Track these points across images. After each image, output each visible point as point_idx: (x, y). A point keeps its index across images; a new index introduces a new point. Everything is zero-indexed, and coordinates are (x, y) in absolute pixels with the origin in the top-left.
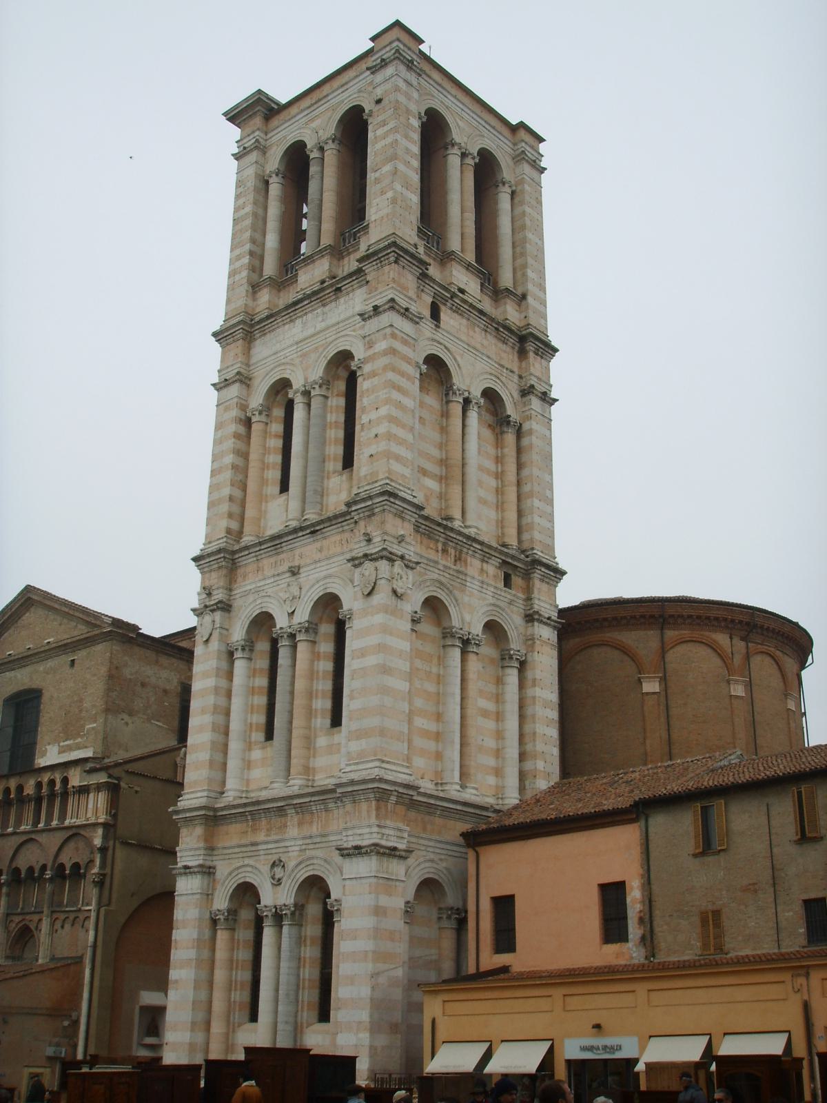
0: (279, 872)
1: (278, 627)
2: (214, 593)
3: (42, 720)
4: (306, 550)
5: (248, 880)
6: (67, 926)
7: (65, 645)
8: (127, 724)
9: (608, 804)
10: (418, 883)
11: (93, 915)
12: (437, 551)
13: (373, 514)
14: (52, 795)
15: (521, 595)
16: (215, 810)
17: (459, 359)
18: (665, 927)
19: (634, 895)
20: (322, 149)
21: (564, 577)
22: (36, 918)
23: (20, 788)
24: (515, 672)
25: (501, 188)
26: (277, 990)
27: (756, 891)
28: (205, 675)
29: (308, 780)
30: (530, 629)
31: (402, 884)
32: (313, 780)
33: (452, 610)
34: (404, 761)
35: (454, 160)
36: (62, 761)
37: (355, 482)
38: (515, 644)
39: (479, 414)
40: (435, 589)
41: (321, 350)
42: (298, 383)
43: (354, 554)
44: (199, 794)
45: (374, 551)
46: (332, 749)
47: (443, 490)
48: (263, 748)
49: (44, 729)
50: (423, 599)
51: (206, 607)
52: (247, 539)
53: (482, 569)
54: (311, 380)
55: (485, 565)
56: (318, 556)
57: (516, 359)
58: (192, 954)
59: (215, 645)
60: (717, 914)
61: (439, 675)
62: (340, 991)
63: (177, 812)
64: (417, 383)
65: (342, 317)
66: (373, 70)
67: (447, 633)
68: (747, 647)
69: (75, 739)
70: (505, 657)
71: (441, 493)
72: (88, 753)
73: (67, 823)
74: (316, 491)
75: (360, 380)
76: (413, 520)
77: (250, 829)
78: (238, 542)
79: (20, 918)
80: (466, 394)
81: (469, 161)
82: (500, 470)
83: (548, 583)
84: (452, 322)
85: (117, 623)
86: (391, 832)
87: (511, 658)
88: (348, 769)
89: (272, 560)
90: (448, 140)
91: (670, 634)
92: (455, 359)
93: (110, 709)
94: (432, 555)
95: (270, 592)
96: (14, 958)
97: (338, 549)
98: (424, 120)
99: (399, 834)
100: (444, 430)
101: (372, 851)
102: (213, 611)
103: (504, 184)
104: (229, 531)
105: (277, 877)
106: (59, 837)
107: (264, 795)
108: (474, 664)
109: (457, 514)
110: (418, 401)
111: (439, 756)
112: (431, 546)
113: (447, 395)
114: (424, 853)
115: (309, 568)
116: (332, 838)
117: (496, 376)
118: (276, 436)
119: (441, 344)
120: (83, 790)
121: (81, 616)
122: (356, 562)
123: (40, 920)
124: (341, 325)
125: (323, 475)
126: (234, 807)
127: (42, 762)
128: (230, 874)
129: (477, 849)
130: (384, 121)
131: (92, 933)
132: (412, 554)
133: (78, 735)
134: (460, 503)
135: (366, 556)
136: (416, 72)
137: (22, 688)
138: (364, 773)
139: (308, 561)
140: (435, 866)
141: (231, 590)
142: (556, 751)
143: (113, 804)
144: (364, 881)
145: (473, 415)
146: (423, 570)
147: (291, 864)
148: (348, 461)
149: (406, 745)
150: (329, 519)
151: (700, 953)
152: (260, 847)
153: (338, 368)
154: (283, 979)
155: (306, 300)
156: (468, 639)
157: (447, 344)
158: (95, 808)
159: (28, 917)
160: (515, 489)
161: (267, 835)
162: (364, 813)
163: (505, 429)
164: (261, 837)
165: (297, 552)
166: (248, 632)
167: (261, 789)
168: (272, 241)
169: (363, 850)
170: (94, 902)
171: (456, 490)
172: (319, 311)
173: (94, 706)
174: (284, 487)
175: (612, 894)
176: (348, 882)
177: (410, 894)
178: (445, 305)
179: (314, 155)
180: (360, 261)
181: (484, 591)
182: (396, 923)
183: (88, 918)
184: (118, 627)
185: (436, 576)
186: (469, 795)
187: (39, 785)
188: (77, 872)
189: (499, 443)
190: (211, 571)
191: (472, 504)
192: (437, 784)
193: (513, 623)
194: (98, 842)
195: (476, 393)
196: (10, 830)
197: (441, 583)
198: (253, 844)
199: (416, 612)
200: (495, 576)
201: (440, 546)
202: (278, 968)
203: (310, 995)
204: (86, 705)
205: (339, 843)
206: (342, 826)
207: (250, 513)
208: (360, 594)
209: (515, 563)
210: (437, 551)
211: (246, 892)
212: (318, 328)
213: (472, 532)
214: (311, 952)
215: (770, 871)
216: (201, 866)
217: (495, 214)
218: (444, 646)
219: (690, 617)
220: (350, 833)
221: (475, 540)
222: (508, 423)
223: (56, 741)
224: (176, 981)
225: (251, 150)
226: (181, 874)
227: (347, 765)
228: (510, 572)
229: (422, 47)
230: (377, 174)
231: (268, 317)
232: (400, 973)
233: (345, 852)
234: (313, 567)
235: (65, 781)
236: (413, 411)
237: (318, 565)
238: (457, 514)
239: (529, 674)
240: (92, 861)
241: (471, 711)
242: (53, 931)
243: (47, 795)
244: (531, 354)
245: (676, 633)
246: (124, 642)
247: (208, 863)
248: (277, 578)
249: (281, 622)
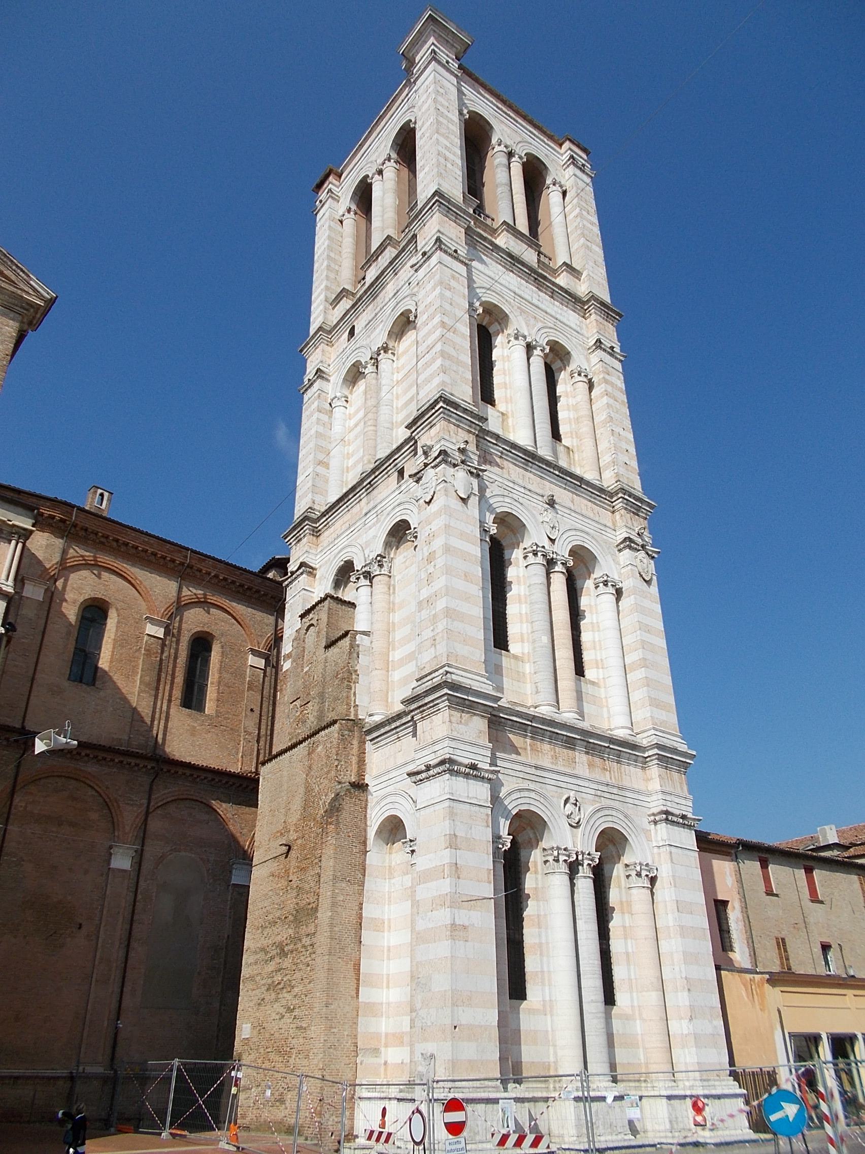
60: (783, 939)
77: (529, 748)
155: (527, 268)
237: (573, 514)
248: (528, 493)
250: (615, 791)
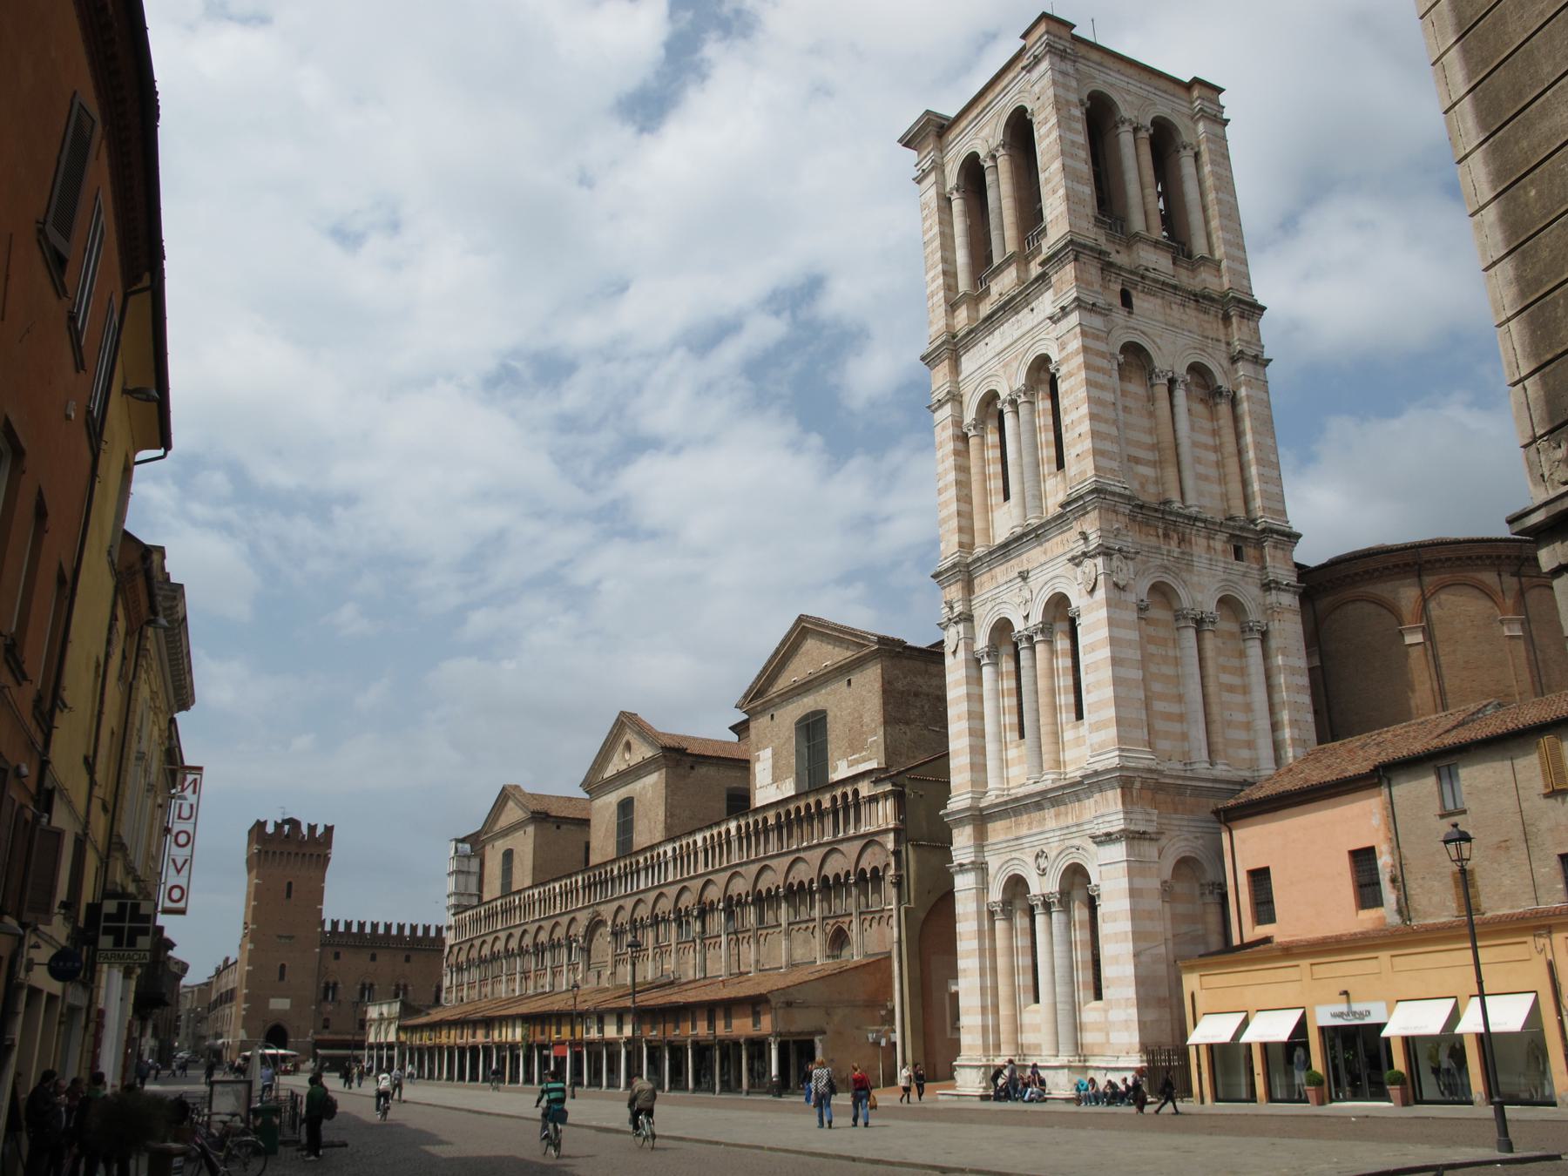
0: (1043, 863)
1: (1016, 631)
2: (955, 605)
3: (829, 738)
4: (1032, 557)
5: (1017, 872)
6: (874, 925)
7: (840, 667)
8: (905, 733)
9: (1352, 770)
10: (1174, 862)
11: (895, 913)
12: (1158, 537)
13: (1087, 513)
14: (846, 808)
15: (1255, 566)
16: (981, 810)
17: (1158, 340)
18: (1419, 890)
19: (1384, 861)
20: (994, 157)
21: (1300, 540)
22: (847, 919)
23: (819, 803)
24: (1257, 643)
25: (1183, 153)
26: (1053, 973)
27: (1508, 848)
28: (957, 684)
29: (1061, 774)
30: (1269, 598)
31: (1156, 866)
32: (1066, 774)
33: (1182, 592)
34: (1145, 746)
35: (1126, 137)
36: (850, 774)
37: (1068, 482)
38: (1254, 615)
39: (1188, 391)
40: (1159, 574)
41: (1020, 357)
42: (1004, 394)
43: (1074, 553)
44: (965, 796)
45: (1091, 548)
46: (1079, 742)
47: (1159, 475)
48: (1018, 746)
49: (833, 746)
50: (1149, 586)
51: (950, 620)
52: (979, 551)
53: (1209, 546)
54: (1015, 388)
55: (1211, 542)
56: (1043, 559)
57: (1221, 326)
58: (974, 944)
59: (961, 654)
61: (1176, 658)
62: (1107, 972)
63: (948, 815)
64: (1116, 374)
65: (1035, 323)
66: (1029, 69)
67: (1179, 615)
68: (1520, 583)
69: (861, 752)
70: (1245, 629)
71: (1157, 478)
72: (873, 765)
73: (862, 831)
74: (1034, 496)
75: (1059, 381)
76: (1127, 511)
78: (971, 554)
80: (1170, 375)
81: (1144, 134)
82: (1218, 443)
83: (1283, 549)
84: (1146, 305)
85: (882, 640)
86: (1139, 817)
87: (1251, 629)
88: (1092, 760)
89: (1003, 568)
90: (1117, 119)
91: (1427, 580)
92: (1154, 342)
93: (888, 721)
94: (1153, 541)
95: (1005, 598)
96: (833, 957)
97: (1061, 551)
98: (1088, 105)
99: (1148, 817)
100: (1152, 415)
101: (1121, 837)
102: (956, 623)
103: (1185, 148)
104: (961, 545)
105: (1042, 867)
106: (859, 844)
107: (1021, 792)
108: (1210, 642)
109: (1174, 496)
110: (1119, 393)
111: (1184, 737)
112: (1151, 532)
113: (1150, 378)
114: (1178, 833)
115: (1037, 571)
116: (1086, 827)
117: (1200, 349)
118: (993, 447)
119: (1136, 329)
120: (873, 799)
121: (850, 638)
122: (1076, 561)
123: (851, 921)
124: (1035, 330)
125: (1038, 479)
126: (997, 805)
127: (835, 776)
128: (1000, 868)
129: (1229, 824)
130: (1046, 118)
131: (895, 930)
132: (1130, 544)
133: (863, 749)
134: (1177, 484)
135: (1085, 554)
136: (1070, 59)
137: (809, 711)
138: (1106, 762)
139: (1036, 565)
140: (1190, 844)
141: (970, 601)
142: (1310, 717)
143: (900, 808)
144: (1118, 865)
145: (1180, 394)
146: (1144, 558)
147: (1052, 855)
148: (1060, 464)
149: (1145, 730)
150: (1048, 522)
151: (1456, 914)
152: (1024, 841)
153: (1039, 372)
154: (1057, 962)
156: (1202, 618)
157: (1143, 328)
158: (884, 815)
160: (1236, 459)
161: (1029, 829)
162: (1112, 802)
163: (1218, 401)
164: (1024, 831)
165: (1024, 557)
166: (991, 638)
167: (1020, 786)
168: (961, 257)
169: (1114, 837)
170: (894, 902)
171: (1171, 473)
172: (1013, 319)
173: (872, 720)
174: (1007, 497)
175: (1363, 859)
176: (1103, 868)
177: (1167, 873)
178: (1135, 289)
179: (988, 164)
180: (1042, 264)
181: (1214, 567)
182: (1154, 903)
183: (891, 916)
184: (884, 644)
185: (1159, 562)
186: (1221, 770)
187: (834, 799)
188: (877, 876)
189: (1213, 416)
190: (950, 585)
191: (1189, 483)
192: (1185, 764)
193: (1250, 594)
194: (891, 846)
195: (1181, 370)
196: (815, 842)
197: (1166, 568)
198: (1017, 839)
199: (1142, 601)
200: (1224, 551)
201: (1161, 532)
202: (1052, 952)
203: (1083, 976)
204: (866, 719)
205: (1093, 831)
206: (1093, 814)
207: (978, 524)
208: (1084, 592)
209: (1245, 534)
210: (1158, 537)
211: (1016, 885)
212: (1015, 337)
213: (1194, 510)
214: (1080, 935)
215: (1521, 827)
216: (972, 863)
217: (1179, 182)
218: (1178, 629)
219: (1448, 559)
220: (1100, 820)
221: (1196, 519)
222: (1221, 394)
223: (845, 756)
224: (965, 970)
225: (930, 172)
226: (957, 872)
227: (1091, 757)
228: (1240, 544)
229: (1074, 32)
230: (1047, 174)
231: (968, 333)
232: (1162, 950)
233: (1098, 840)
234: (1040, 569)
235: (856, 792)
236: (1114, 404)
238: (1174, 496)
239: (1274, 643)
240: (888, 865)
241: (1212, 689)
242: (862, 931)
244: (1234, 320)
245: (1436, 578)
246: (893, 657)
247: (979, 860)
248: (1010, 584)
249: (1019, 625)
250: (1074, 829)
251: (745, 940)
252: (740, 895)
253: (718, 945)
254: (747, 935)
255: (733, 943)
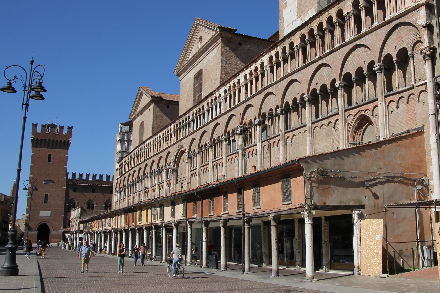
79: (357, 110)
159: (363, 108)
243: (364, 6)
251: (276, 144)
252: (271, 110)
253: (254, 152)
254: (276, 139)
255: (266, 147)
